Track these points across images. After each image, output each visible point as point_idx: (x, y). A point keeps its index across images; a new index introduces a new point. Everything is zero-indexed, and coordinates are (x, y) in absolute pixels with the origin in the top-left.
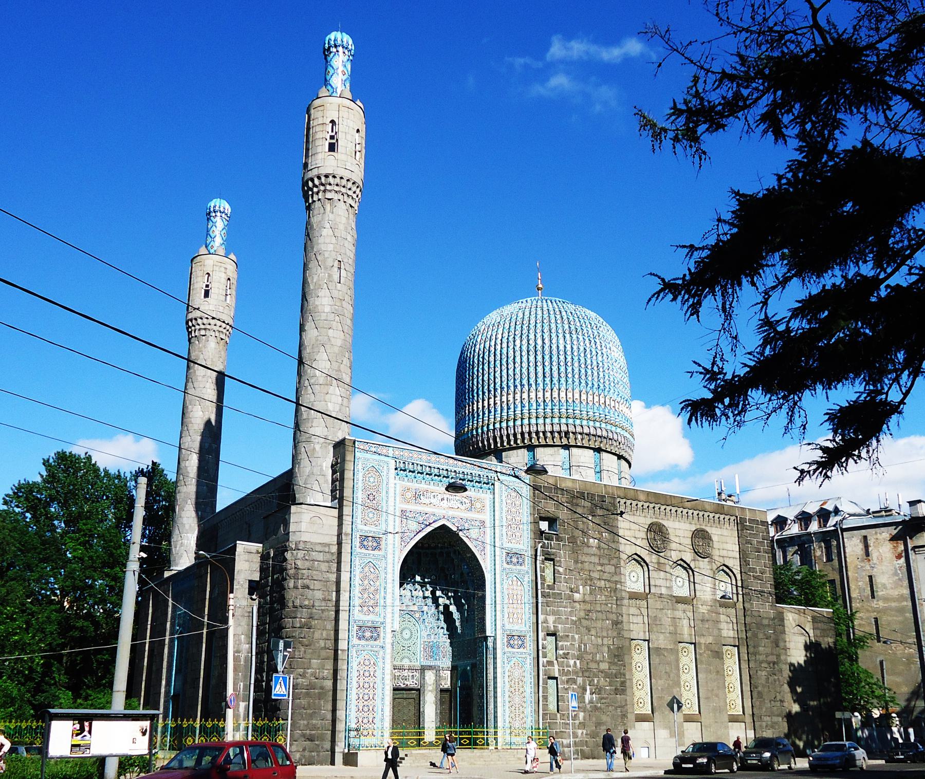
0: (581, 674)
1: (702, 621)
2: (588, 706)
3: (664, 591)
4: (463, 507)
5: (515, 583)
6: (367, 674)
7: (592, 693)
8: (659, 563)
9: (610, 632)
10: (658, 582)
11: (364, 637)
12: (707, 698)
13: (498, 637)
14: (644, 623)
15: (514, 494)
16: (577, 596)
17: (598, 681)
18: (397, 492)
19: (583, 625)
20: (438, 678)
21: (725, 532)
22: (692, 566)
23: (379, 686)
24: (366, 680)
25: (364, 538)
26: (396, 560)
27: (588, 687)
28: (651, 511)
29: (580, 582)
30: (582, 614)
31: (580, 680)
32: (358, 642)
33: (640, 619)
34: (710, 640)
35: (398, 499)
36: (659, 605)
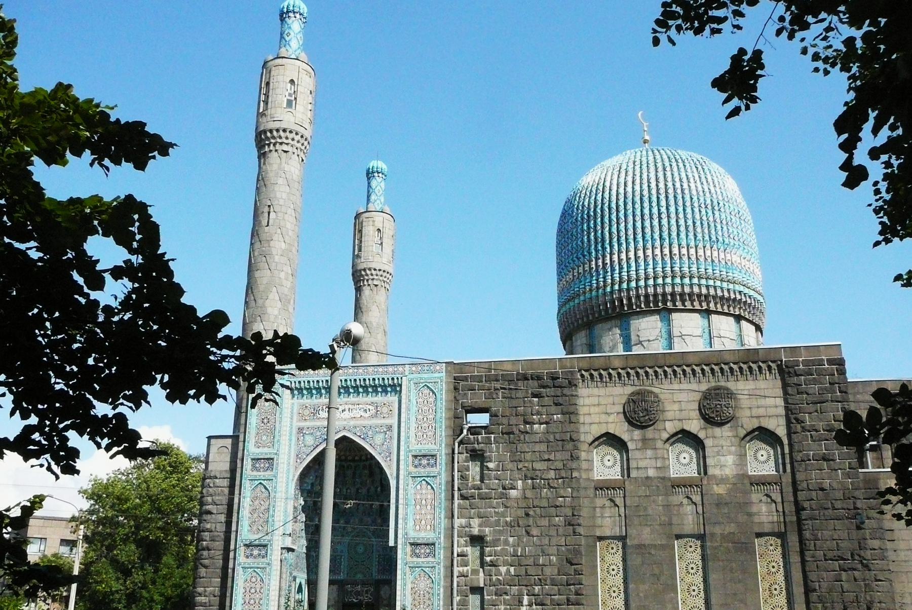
3: (651, 473)
4: (367, 415)
6: (253, 591)
8: (644, 440)
10: (642, 464)
11: (252, 555)
13: (399, 547)
14: (620, 515)
15: (427, 391)
16: (513, 493)
18: (295, 411)
19: (522, 524)
22: (701, 435)
24: (252, 596)
25: (256, 460)
26: (291, 477)
27: (526, 597)
28: (633, 377)
30: (521, 513)
32: (245, 560)
34: (731, 528)
35: (295, 417)
36: (642, 491)
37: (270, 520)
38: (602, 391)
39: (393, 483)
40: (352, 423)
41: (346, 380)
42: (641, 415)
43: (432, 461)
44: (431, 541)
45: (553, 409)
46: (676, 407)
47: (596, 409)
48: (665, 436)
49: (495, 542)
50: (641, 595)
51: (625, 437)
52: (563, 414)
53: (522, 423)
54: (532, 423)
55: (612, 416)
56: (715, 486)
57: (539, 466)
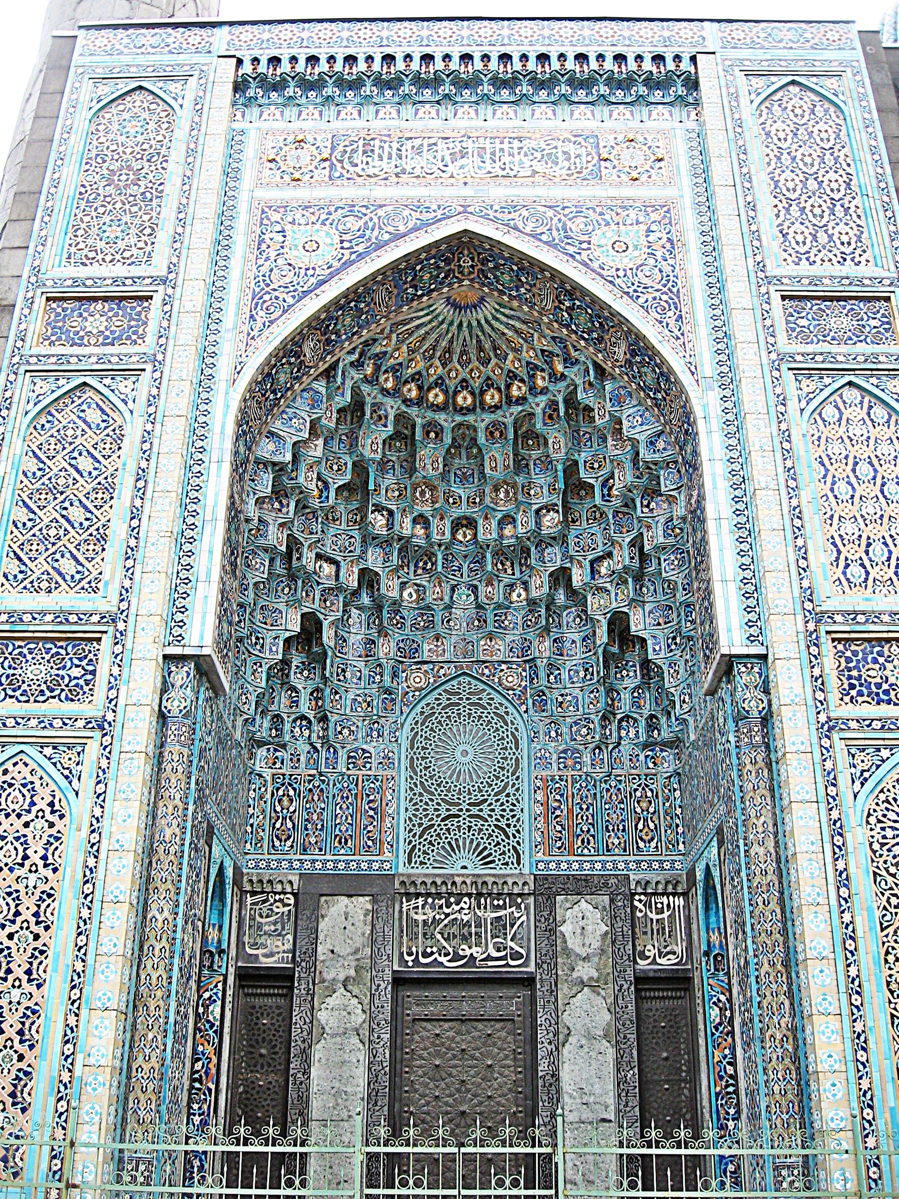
5: (855, 413)
20: (626, 929)
23: (65, 910)
37: (118, 531)
39: (705, 402)
40: (498, 193)
41: (466, 58)
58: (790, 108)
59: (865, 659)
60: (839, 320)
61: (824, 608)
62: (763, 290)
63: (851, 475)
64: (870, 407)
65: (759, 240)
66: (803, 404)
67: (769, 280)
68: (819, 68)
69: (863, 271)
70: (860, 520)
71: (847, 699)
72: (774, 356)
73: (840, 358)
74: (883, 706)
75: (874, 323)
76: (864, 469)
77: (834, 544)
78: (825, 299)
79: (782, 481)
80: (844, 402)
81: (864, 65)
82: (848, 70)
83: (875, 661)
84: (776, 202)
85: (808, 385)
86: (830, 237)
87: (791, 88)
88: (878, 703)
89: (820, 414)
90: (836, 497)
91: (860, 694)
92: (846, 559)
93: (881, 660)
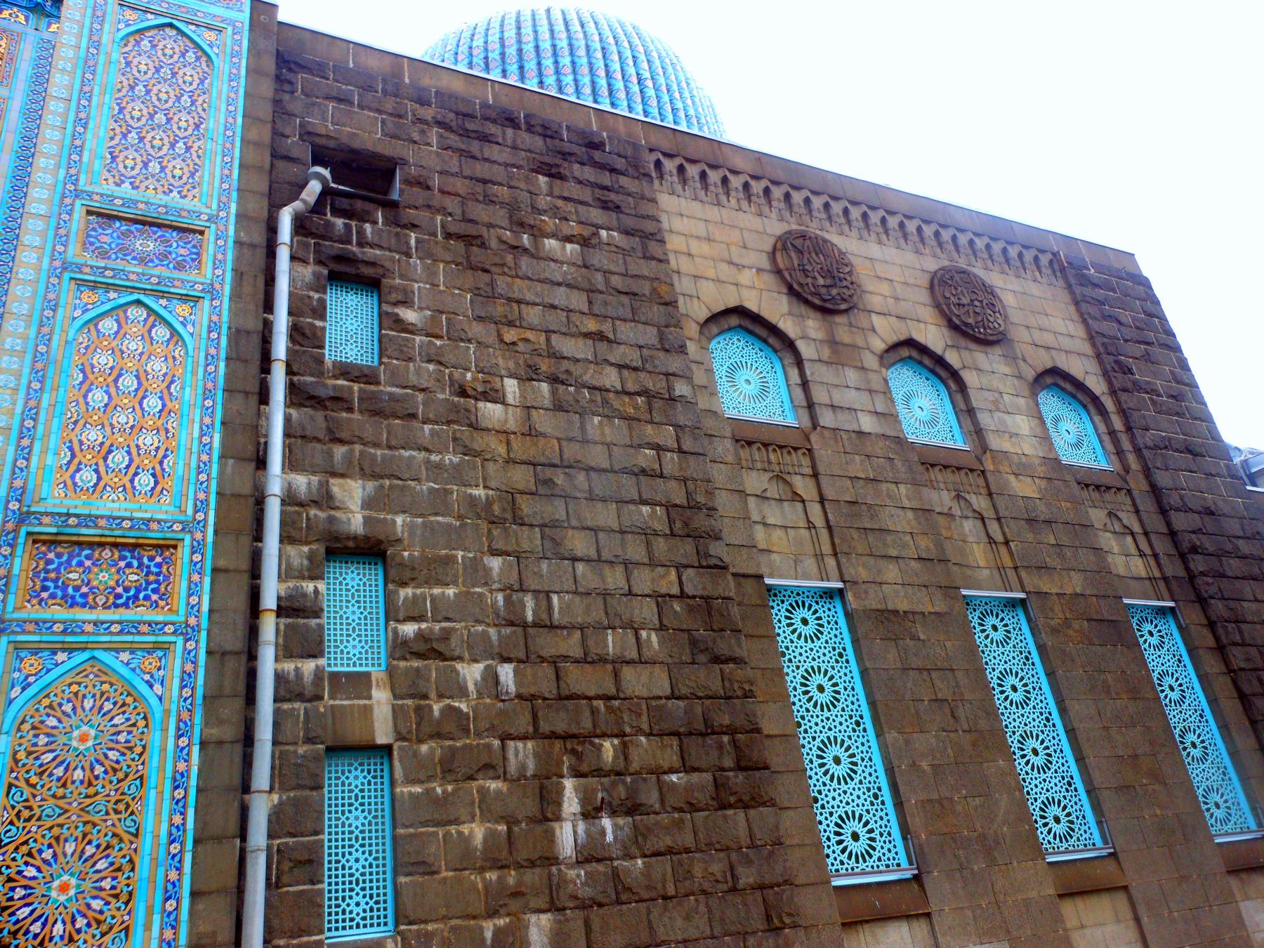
0: (523, 723)
1: (1031, 521)
2: (577, 875)
3: (867, 423)
7: (590, 813)
9: (661, 545)
10: (839, 397)
12: (1124, 788)
14: (811, 526)
16: (491, 412)
17: (624, 751)
21: (1035, 289)
22: (952, 358)
27: (569, 784)
28: (778, 204)
29: (503, 362)
31: (522, 754)
33: (793, 513)
38: (713, 213)
42: (821, 281)
43: (179, 249)
44: (155, 534)
45: (596, 215)
46: (885, 288)
47: (705, 248)
48: (879, 346)
49: (436, 570)
50: (924, 765)
51: (788, 326)
52: (627, 233)
53: (505, 223)
54: (538, 233)
55: (747, 273)
56: (1012, 478)
57: (568, 346)
58: (160, 46)
59: (69, 562)
60: (146, 244)
61: (33, 509)
62: (68, 201)
63: (112, 385)
64: (153, 326)
65: (81, 156)
66: (78, 313)
67: (78, 194)
68: (200, 18)
69: (187, 204)
70: (108, 429)
71: (34, 601)
72: (58, 264)
73: (132, 277)
74: (77, 609)
75: (182, 251)
76: (128, 382)
77: (71, 449)
78: (136, 222)
79: (24, 381)
80: (127, 318)
81: (247, 27)
82: (230, 29)
83: (80, 564)
84: (116, 126)
85: (87, 296)
86: (163, 169)
87: (167, 30)
88: (71, 606)
89: (96, 326)
90: (87, 404)
91: (53, 596)
92: (80, 463)
93: (88, 563)
